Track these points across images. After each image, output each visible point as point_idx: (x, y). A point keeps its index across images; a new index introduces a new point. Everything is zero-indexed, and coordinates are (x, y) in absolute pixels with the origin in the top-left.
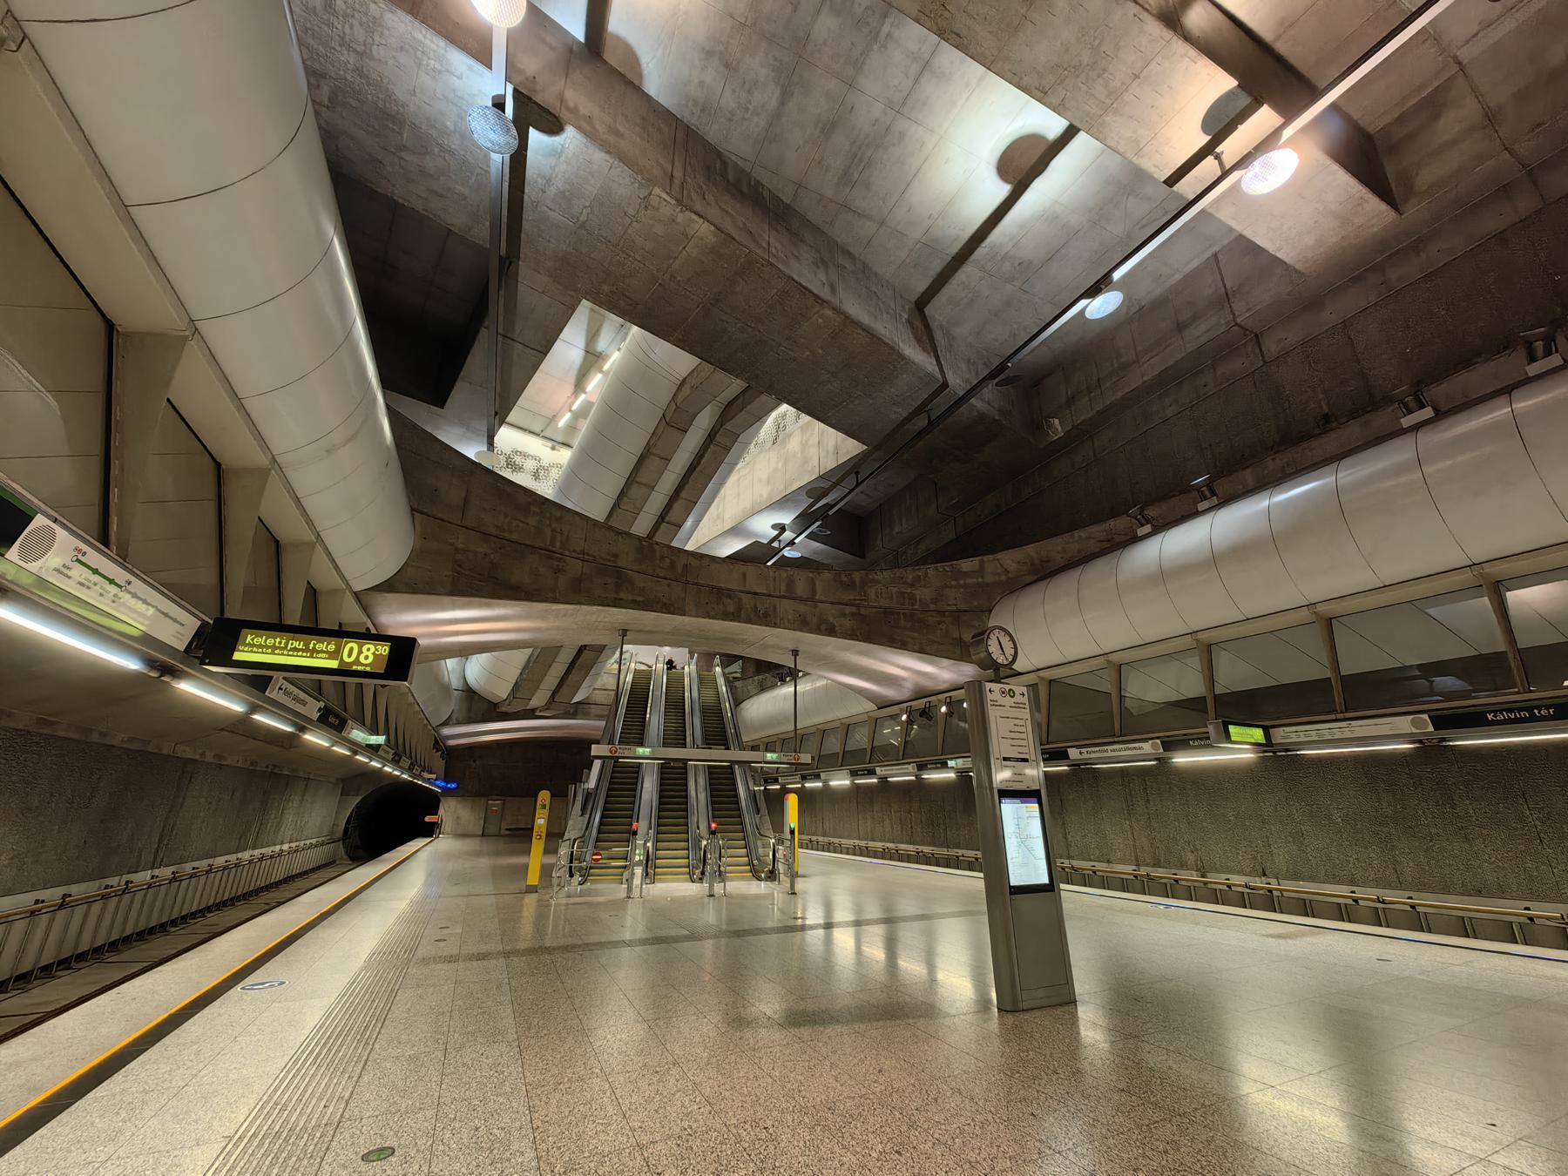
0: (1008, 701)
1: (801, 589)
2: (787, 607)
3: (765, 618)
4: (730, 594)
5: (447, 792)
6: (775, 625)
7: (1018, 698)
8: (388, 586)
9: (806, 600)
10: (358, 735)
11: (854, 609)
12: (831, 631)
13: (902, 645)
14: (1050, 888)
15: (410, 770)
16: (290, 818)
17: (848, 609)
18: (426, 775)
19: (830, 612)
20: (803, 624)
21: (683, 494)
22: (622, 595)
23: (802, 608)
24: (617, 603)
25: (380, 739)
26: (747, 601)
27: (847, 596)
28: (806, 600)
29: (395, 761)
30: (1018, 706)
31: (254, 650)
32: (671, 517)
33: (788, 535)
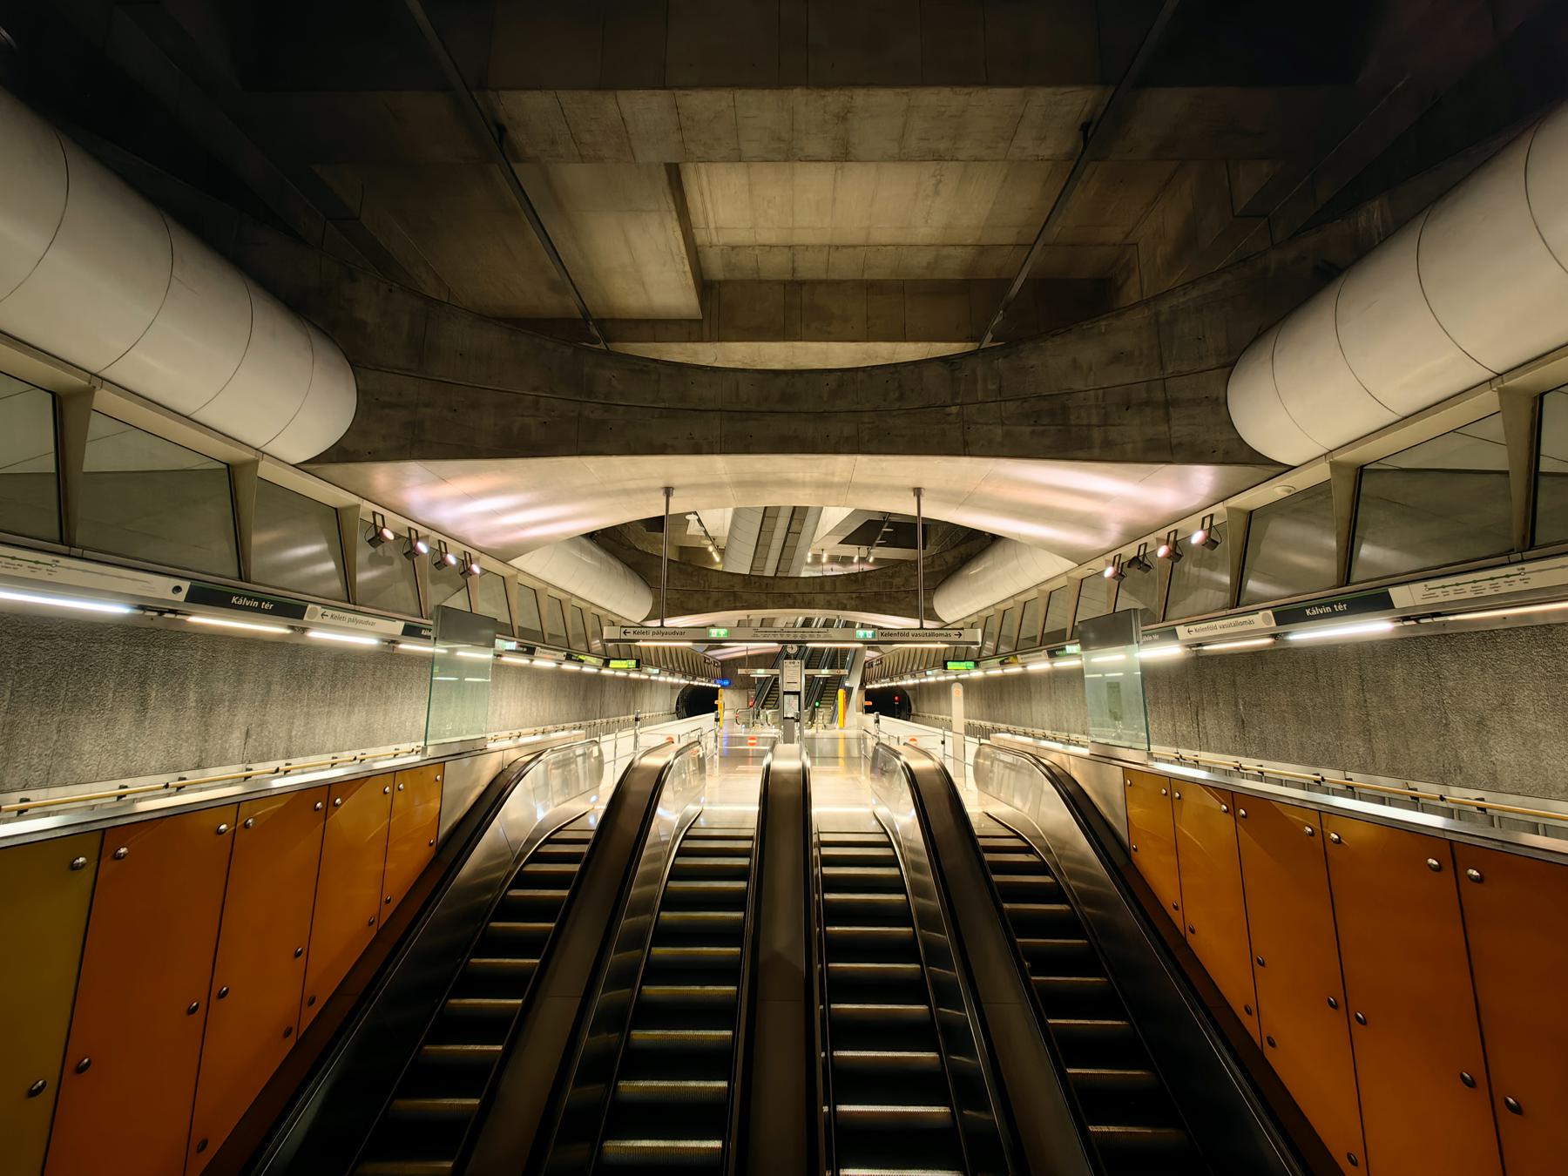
1: (828, 587)
2: (820, 598)
4: (790, 595)
5: (723, 687)
8: (647, 619)
10: (650, 670)
13: (885, 613)
15: (684, 677)
16: (646, 701)
19: (843, 597)
20: (829, 606)
23: (828, 597)
24: (735, 609)
26: (799, 597)
27: (854, 588)
29: (672, 673)
31: (613, 664)
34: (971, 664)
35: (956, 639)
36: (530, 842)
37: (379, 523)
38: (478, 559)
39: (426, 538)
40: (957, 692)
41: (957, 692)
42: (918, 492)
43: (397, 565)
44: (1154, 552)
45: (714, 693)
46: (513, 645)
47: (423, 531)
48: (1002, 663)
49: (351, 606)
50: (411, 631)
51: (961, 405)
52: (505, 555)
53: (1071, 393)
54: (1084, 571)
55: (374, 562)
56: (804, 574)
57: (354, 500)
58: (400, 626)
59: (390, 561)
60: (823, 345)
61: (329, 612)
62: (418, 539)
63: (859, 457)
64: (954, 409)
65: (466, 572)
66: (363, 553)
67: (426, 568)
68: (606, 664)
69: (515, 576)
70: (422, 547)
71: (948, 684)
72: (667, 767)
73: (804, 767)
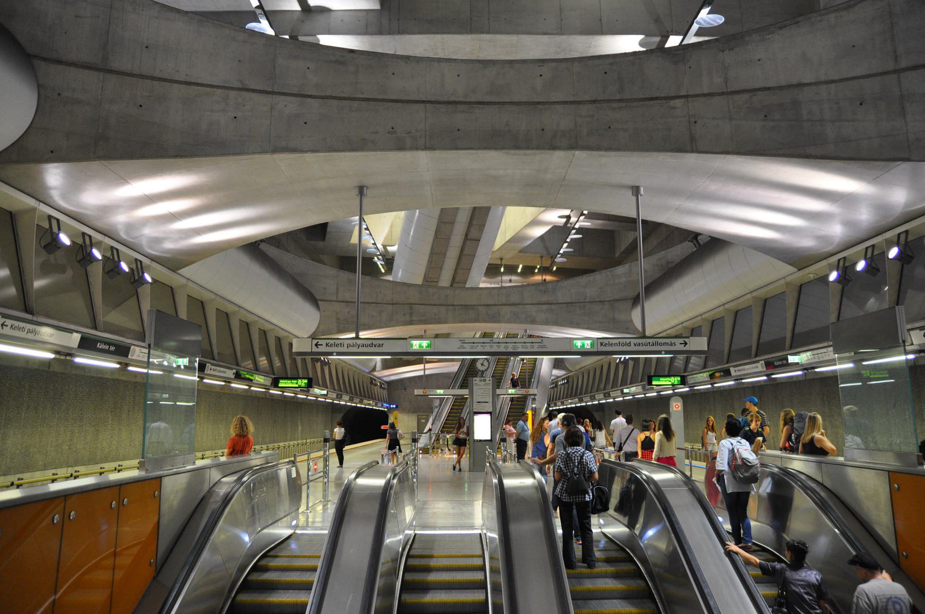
0: (483, 383)
3: (495, 319)
6: (499, 322)
7: (487, 382)
9: (518, 304)
11: (548, 306)
12: (533, 322)
14: (491, 441)
17: (544, 307)
18: (365, 401)
20: (515, 319)
21: (475, 222)
22: (414, 318)
24: (411, 323)
25: (325, 392)
28: (518, 304)
30: (486, 384)
32: (473, 235)
33: (573, 219)
34: (676, 380)
35: (682, 348)
36: (233, 568)
37: (55, 229)
38: (149, 267)
39: (99, 245)
40: (676, 406)
41: (676, 406)
42: (636, 190)
43: (69, 273)
44: (884, 254)
45: (383, 417)
46: (183, 362)
47: (97, 236)
48: (712, 376)
49: (29, 317)
50: (87, 344)
51: (686, 96)
52: (176, 262)
53: (800, 85)
54: (810, 273)
55: (45, 270)
56: (482, 285)
57: (32, 202)
58: (77, 337)
59: (62, 269)
60: (514, 38)
61: (9, 322)
62: (92, 245)
63: (577, 152)
64: (678, 103)
65: (135, 278)
66: (33, 257)
67: (97, 274)
68: (275, 383)
69: (185, 286)
70: (97, 253)
71: (669, 397)
72: (388, 487)
73: (540, 483)
